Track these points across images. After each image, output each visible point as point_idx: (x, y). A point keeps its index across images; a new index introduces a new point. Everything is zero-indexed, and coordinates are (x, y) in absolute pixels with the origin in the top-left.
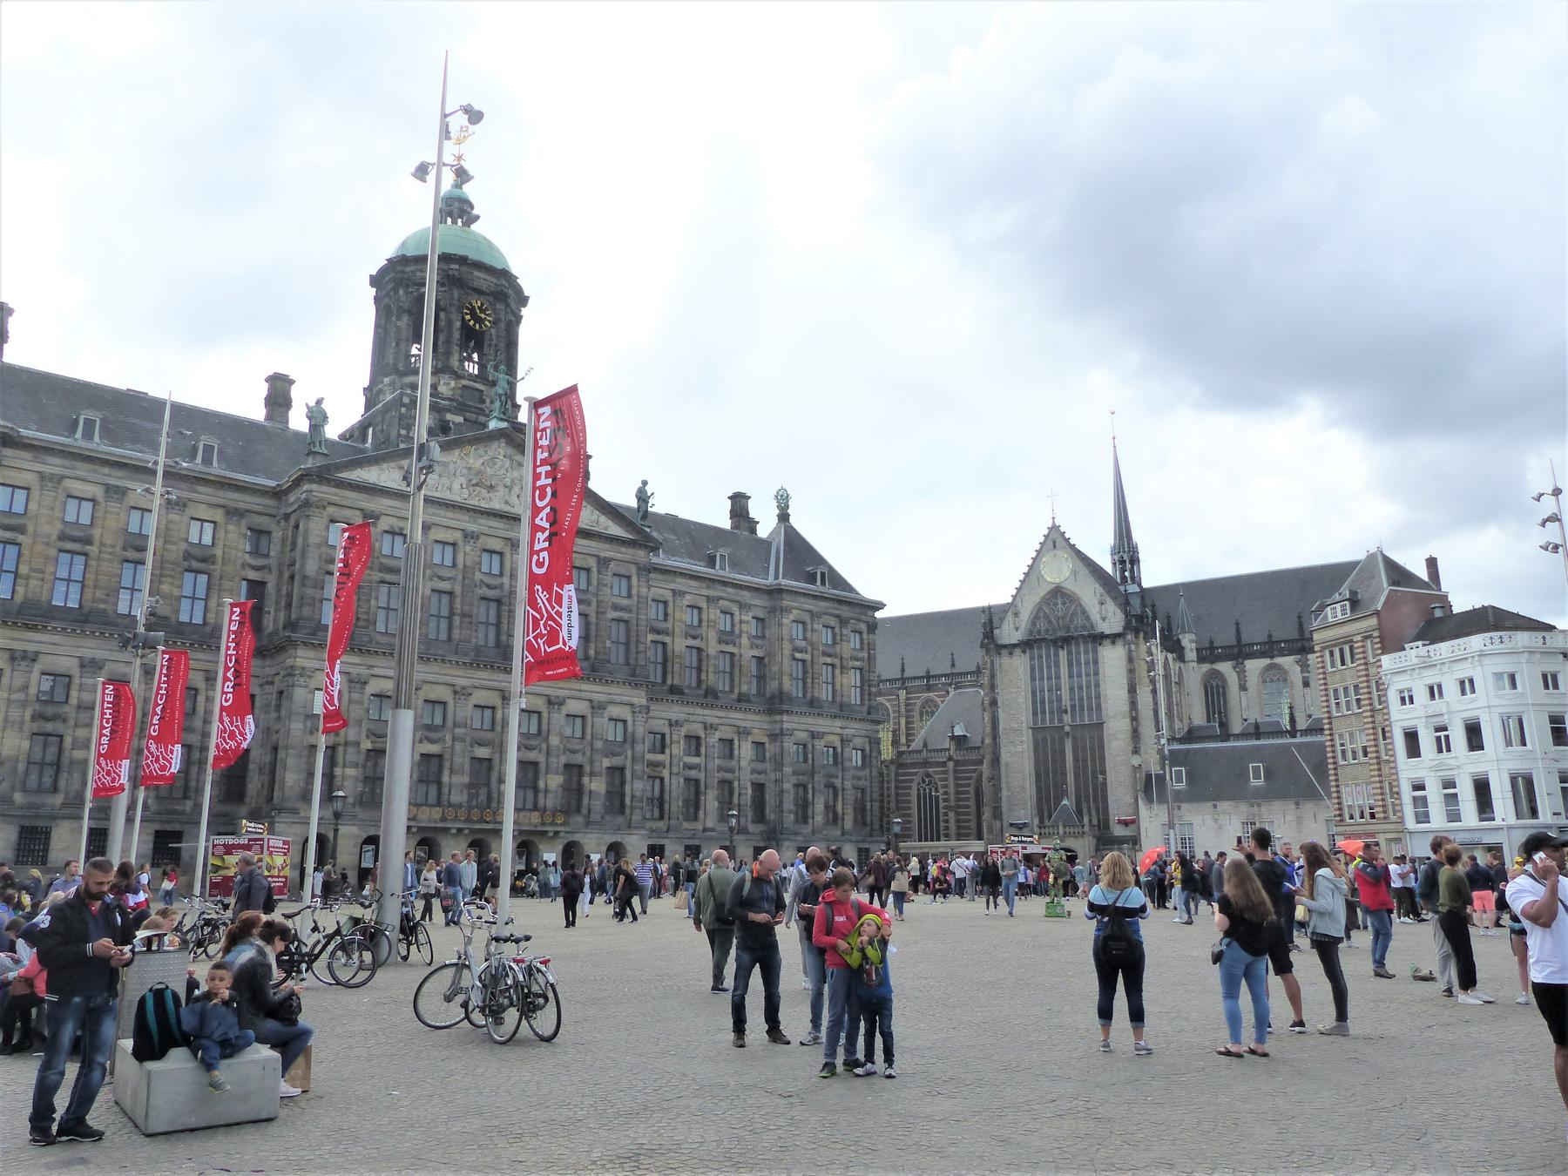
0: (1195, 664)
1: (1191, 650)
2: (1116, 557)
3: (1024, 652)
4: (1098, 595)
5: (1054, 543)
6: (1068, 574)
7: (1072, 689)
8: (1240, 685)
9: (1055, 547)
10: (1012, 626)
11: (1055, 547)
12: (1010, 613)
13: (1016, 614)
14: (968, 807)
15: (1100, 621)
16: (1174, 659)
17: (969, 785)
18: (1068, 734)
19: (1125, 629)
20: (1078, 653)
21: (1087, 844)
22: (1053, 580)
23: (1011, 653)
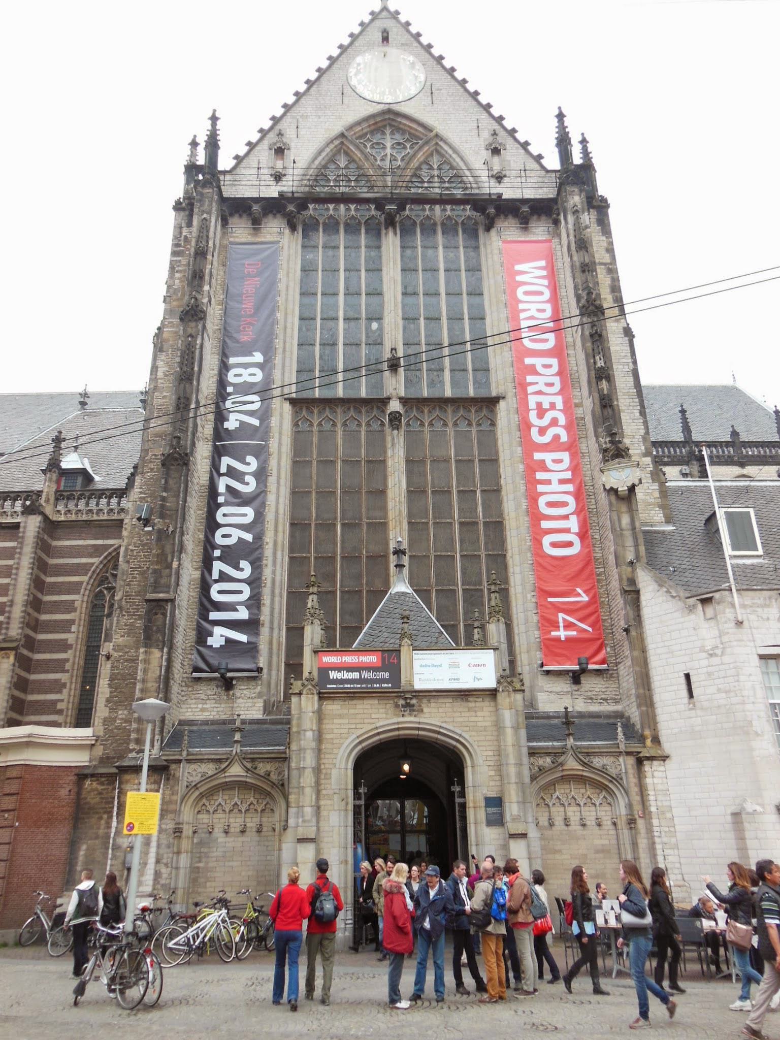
3: (293, 228)
4: (486, 135)
12: (266, 143)
13: (280, 152)
14: (64, 646)
17: (74, 588)
21: (508, 717)
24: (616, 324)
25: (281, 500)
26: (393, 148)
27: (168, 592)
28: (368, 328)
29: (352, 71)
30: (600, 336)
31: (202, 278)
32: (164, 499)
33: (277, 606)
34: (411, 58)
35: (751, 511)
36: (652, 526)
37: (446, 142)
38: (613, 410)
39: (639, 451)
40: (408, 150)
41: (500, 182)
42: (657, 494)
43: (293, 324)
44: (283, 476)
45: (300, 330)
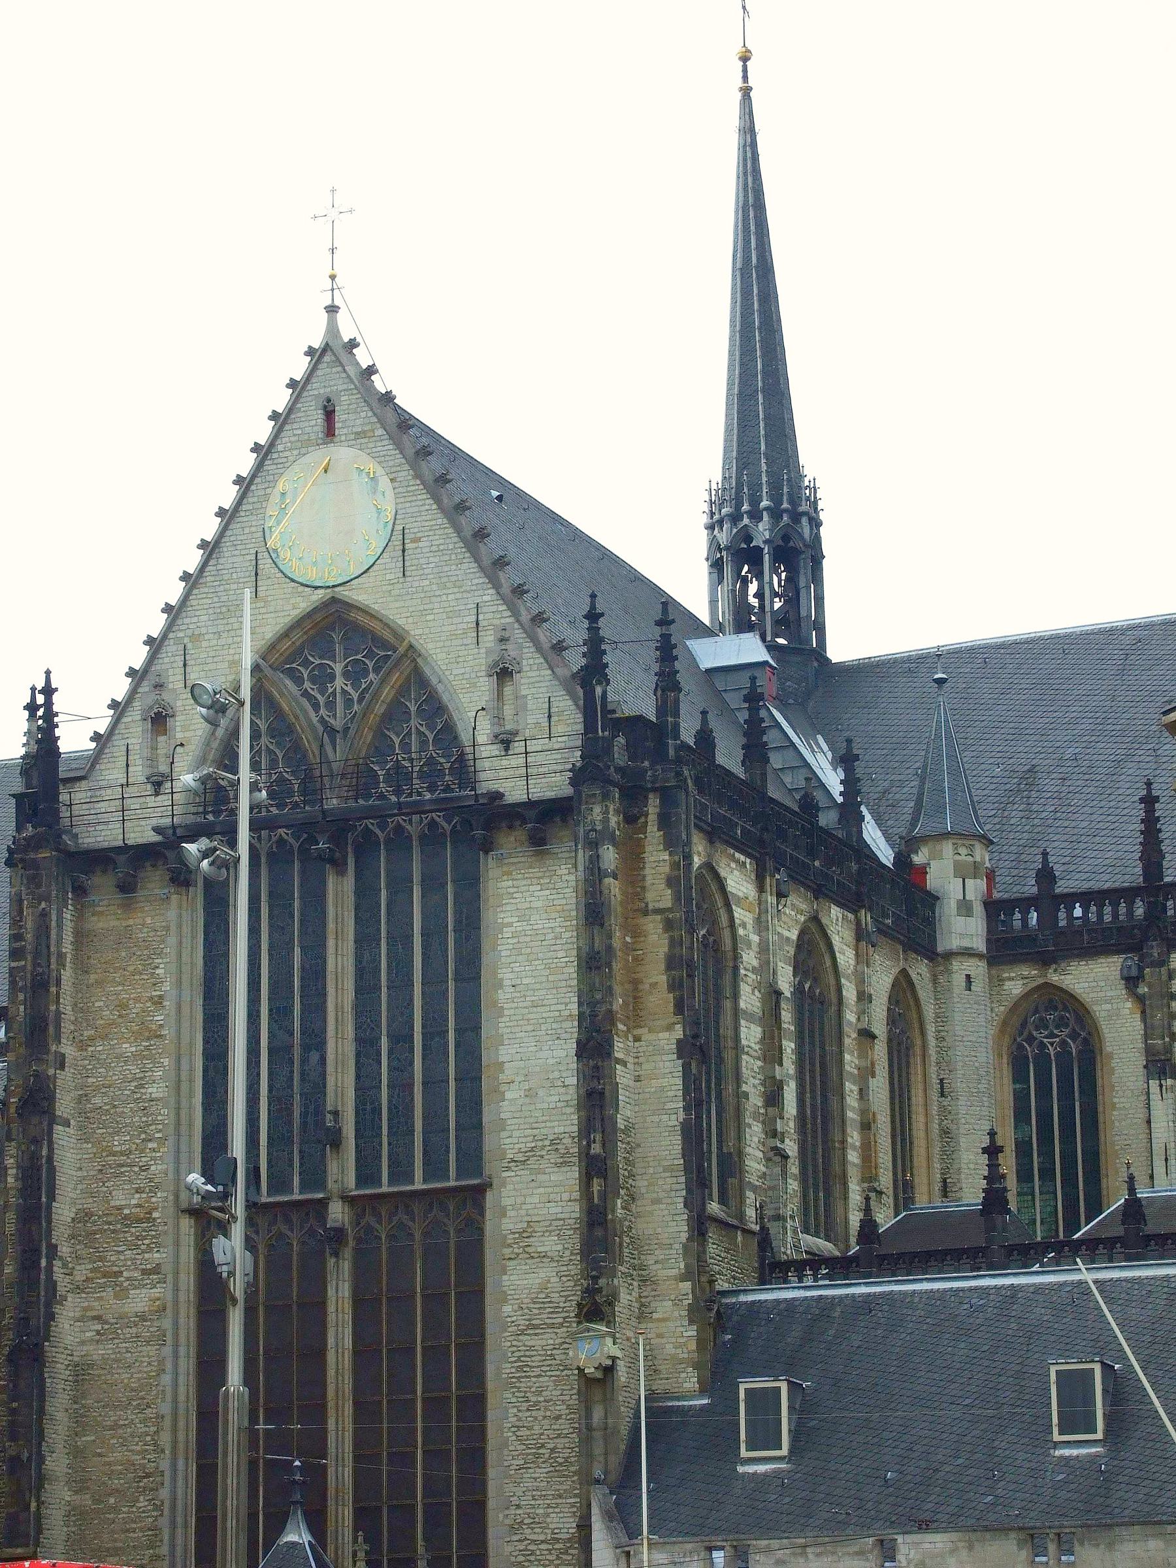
0: (977, 968)
1: (965, 907)
2: (723, 537)
4: (489, 639)
5: (329, 415)
6: (377, 545)
7: (366, 1045)
8: (1149, 1051)
9: (330, 432)
10: (139, 772)
11: (330, 432)
12: (134, 715)
13: (159, 720)
15: (487, 750)
16: (860, 935)
18: (337, 1236)
19: (579, 777)
20: (400, 886)
22: (312, 576)
23: (127, 887)
24: (666, 1035)
25: (182, 1379)
26: (346, 674)
27: (27, 1545)
28: (304, 1061)
29: (272, 510)
30: (602, 1094)
31: (44, 1030)
32: (13, 1412)
33: (179, 1541)
34: (372, 466)
35: (784, 1387)
36: (678, 1399)
37: (425, 659)
38: (606, 1230)
39: (675, 1272)
40: (372, 676)
41: (507, 749)
42: (693, 1346)
43: (192, 1070)
44: (183, 1339)
45: (205, 1070)
